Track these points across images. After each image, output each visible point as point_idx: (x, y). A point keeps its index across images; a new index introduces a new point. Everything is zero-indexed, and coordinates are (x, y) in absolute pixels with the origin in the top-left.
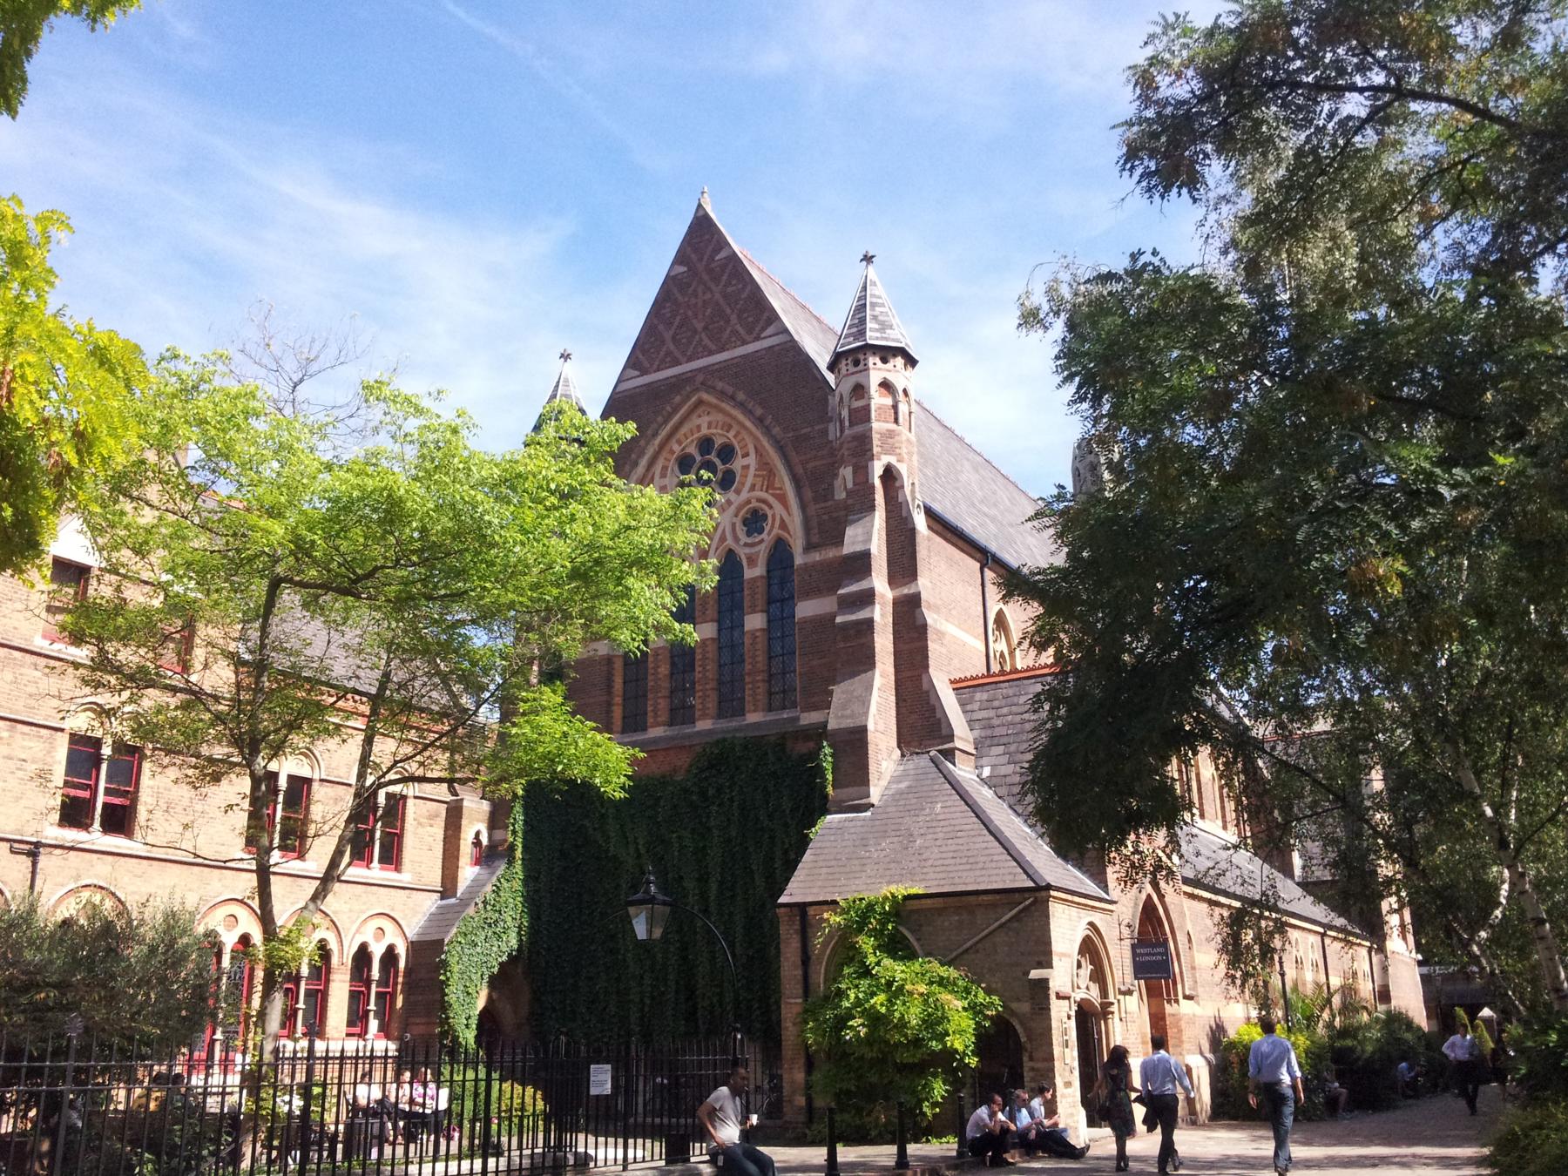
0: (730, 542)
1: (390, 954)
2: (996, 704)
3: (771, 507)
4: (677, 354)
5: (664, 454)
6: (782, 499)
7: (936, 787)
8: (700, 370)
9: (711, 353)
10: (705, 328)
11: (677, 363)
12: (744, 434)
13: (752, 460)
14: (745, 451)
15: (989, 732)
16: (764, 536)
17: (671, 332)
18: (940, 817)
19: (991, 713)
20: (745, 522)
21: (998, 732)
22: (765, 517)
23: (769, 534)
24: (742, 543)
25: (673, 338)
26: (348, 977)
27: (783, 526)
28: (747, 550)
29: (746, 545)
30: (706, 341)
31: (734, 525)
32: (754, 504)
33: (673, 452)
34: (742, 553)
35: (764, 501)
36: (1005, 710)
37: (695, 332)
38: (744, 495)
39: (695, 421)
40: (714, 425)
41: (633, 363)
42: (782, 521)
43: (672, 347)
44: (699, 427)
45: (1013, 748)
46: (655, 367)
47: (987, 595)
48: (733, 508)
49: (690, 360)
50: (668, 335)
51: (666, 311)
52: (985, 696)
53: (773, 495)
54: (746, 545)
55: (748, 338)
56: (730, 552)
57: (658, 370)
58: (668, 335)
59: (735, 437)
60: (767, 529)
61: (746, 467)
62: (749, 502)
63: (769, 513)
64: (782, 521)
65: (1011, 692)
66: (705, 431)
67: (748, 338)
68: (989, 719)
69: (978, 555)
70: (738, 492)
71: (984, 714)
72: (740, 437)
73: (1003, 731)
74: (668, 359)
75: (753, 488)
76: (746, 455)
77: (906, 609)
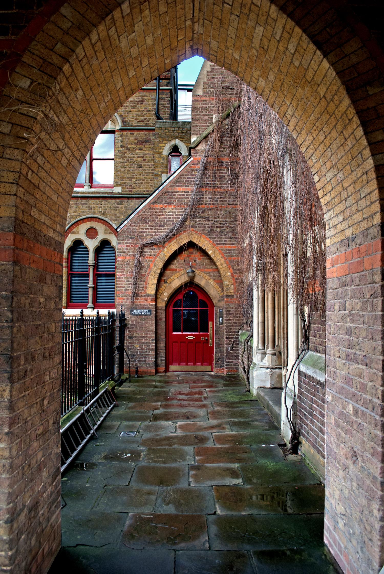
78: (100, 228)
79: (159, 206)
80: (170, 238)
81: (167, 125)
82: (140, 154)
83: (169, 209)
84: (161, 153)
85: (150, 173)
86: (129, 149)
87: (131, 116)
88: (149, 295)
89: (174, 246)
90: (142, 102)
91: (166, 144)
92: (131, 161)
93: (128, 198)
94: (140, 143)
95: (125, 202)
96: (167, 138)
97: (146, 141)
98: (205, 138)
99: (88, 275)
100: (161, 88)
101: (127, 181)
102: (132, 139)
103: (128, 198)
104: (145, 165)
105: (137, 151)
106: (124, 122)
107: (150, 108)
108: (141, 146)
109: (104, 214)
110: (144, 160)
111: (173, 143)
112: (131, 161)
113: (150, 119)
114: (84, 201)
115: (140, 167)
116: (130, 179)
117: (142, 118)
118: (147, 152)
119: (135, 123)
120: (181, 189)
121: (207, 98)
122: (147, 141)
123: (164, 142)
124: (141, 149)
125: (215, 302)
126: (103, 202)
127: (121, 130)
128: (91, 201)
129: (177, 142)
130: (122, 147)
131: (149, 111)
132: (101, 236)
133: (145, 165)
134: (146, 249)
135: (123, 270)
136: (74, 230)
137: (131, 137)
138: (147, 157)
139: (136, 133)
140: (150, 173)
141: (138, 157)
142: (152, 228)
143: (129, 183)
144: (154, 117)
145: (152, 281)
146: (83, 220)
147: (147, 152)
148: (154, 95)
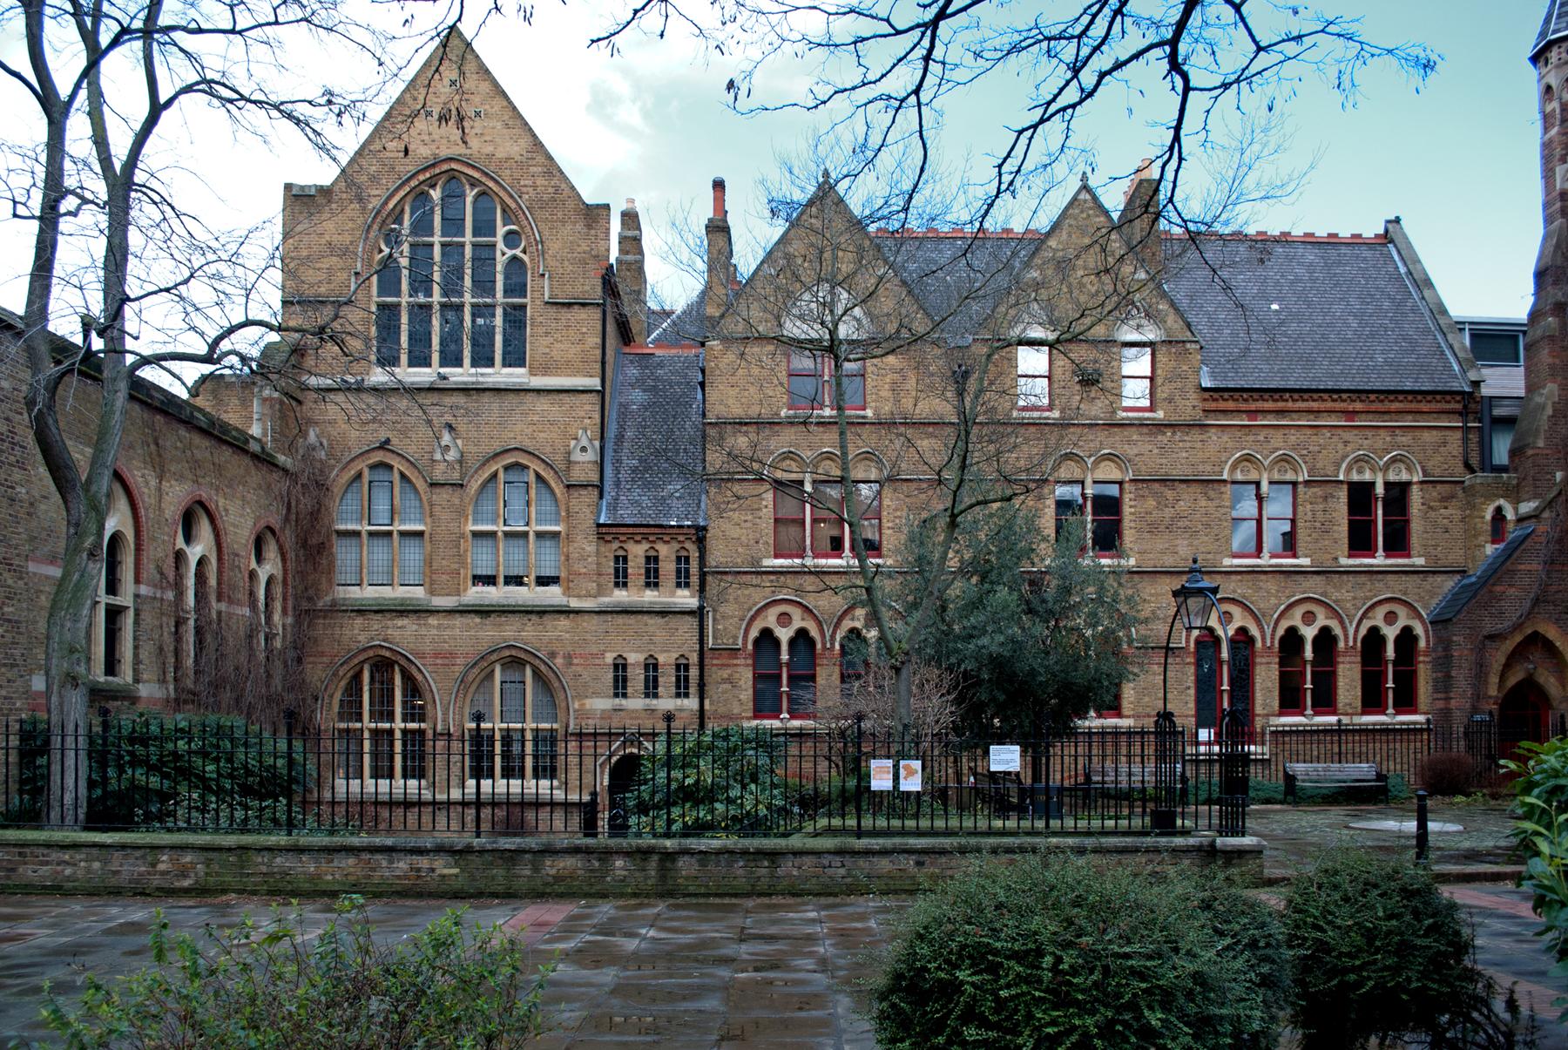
1: (1406, 637)
26: (1359, 659)
78: (1401, 611)
79: (1498, 588)
80: (1517, 627)
81: (1490, 480)
83: (1512, 591)
84: (1483, 517)
86: (1431, 508)
87: (1431, 463)
88: (1490, 697)
89: (1518, 638)
90: (1445, 444)
92: (1435, 524)
93: (1434, 573)
94: (1445, 499)
95: (1430, 579)
96: (1490, 497)
98: (1550, 502)
99: (779, 676)
101: (1431, 549)
102: (1435, 494)
103: (1434, 573)
106: (1425, 473)
107: (1455, 453)
109: (1405, 594)
111: (1497, 504)
112: (1435, 524)
114: (1380, 576)
116: (1436, 546)
119: (1437, 471)
120: (1523, 567)
121: (1548, 452)
124: (1446, 508)
125: (1555, 704)
126: (1404, 578)
127: (1422, 482)
128: (1390, 577)
129: (1502, 502)
130: (1423, 504)
132: (1401, 623)
134: (1487, 642)
135: (1460, 667)
136: (1370, 615)
137: (1434, 492)
139: (1439, 487)
142: (1491, 615)
143: (1434, 552)
144: (1461, 465)
145: (1494, 680)
146: (1380, 602)
148: (1459, 435)
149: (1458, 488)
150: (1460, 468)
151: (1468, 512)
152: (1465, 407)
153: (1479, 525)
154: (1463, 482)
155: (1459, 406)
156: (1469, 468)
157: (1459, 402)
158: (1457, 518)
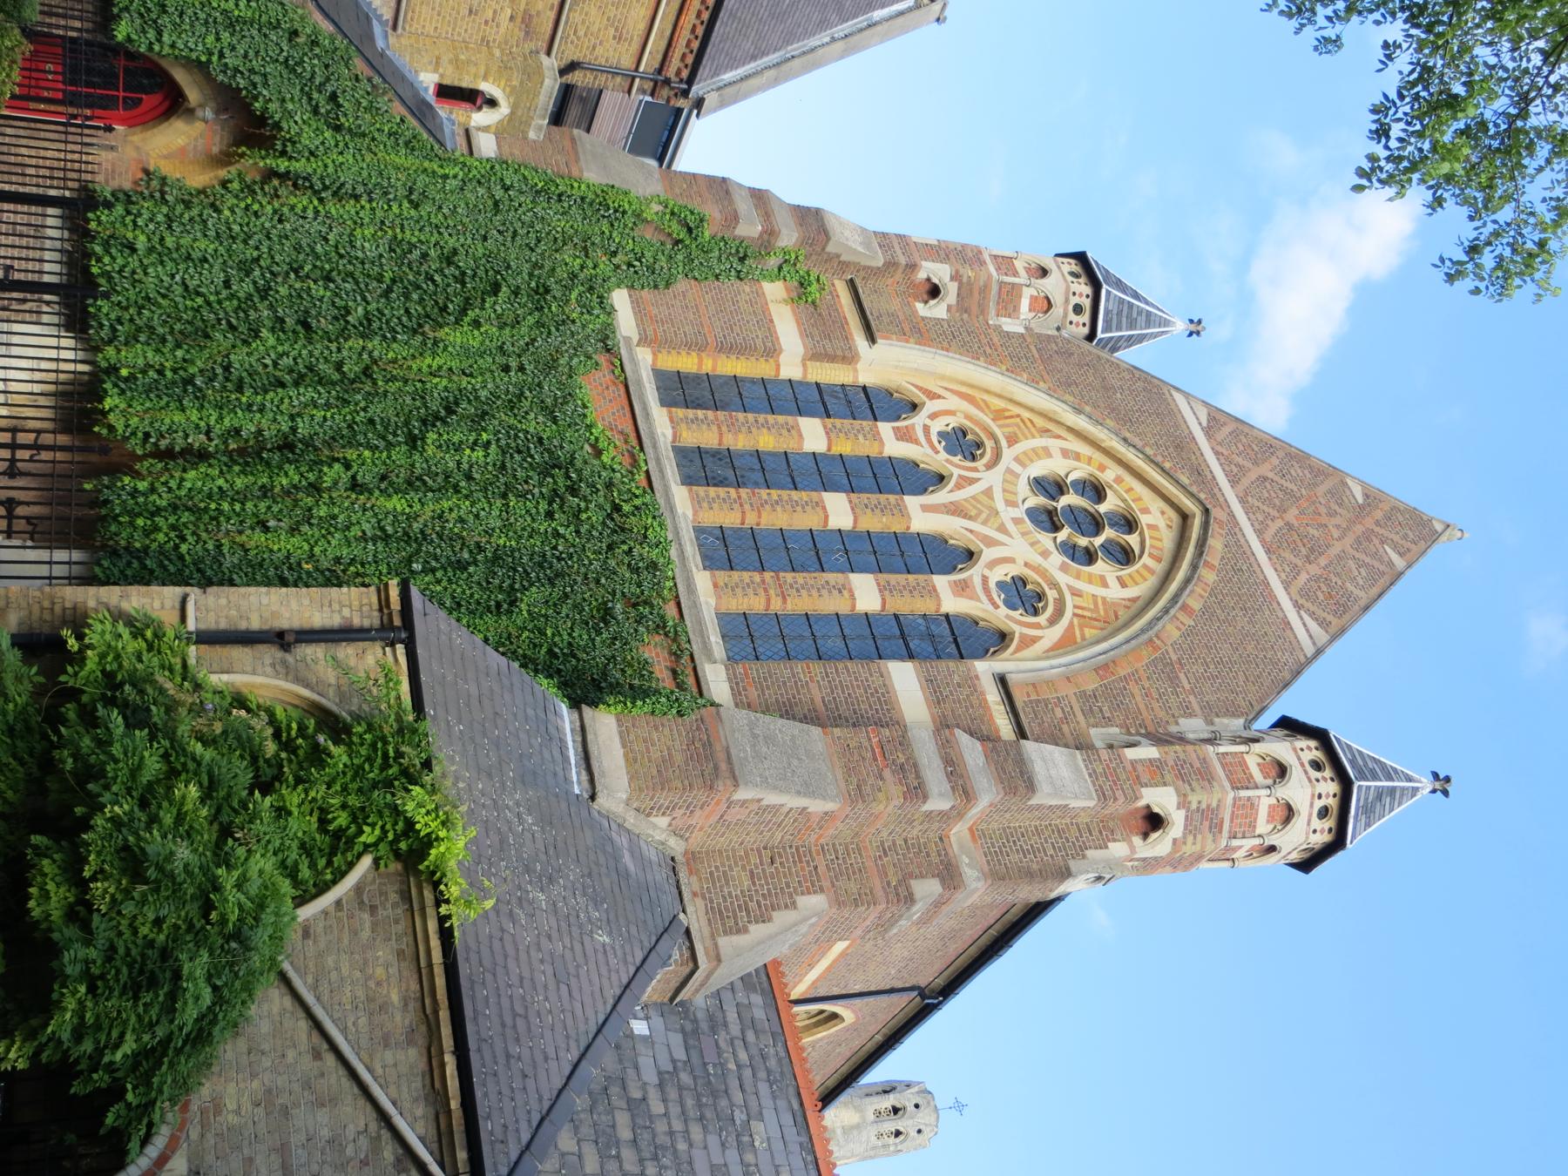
0: (988, 554)
2: (750, 1036)
3: (1053, 621)
4: (1245, 482)
5: (1098, 457)
6: (1067, 643)
7: (633, 930)
8: (1231, 515)
9: (1259, 533)
10: (1289, 526)
11: (1234, 482)
12: (1151, 582)
13: (1115, 593)
14: (1128, 581)
15: (704, 1026)
16: (1004, 610)
17: (1271, 475)
18: (587, 939)
19: (735, 1029)
20: (1020, 581)
21: (707, 1042)
22: (1036, 612)
23: (1007, 616)
24: (987, 572)
25: (1265, 479)
27: (1028, 642)
28: (977, 581)
29: (985, 580)
30: (1274, 527)
31: (1010, 560)
32: (1051, 595)
33: (1102, 468)
34: (974, 573)
35: (1059, 612)
36: (743, 1056)
37: (1283, 510)
38: (1063, 579)
39: (1156, 505)
40: (1155, 534)
41: (1217, 420)
42: (1034, 640)
43: (1253, 476)
44: (1146, 511)
45: (685, 1078)
46: (1219, 448)
47: (871, 999)
48: (1039, 560)
49: (1243, 501)
50: (1265, 470)
51: (1296, 471)
52: (759, 1014)
53: (1071, 624)
54: (985, 580)
55: (1294, 590)
56: (970, 555)
57: (1217, 453)
58: (1265, 470)
59: (1145, 566)
60: (1016, 614)
61: (1105, 584)
62: (1054, 585)
63: (1042, 619)
64: (1034, 640)
65: (772, 1063)
66: (1144, 520)
67: (1294, 590)
68: (725, 1025)
69: (941, 982)
70: (1064, 568)
71: (732, 1016)
72: (1145, 573)
73: (710, 1056)
74: (1235, 470)
75: (1076, 593)
76: (1123, 585)
77: (935, 859)
82: (503, 15)
84: (485, 78)
85: (454, 30)
91: (504, 90)
97: (529, 33)
100: (637, 80)
104: (474, 21)
105: (509, 11)
107: (599, 51)
108: (519, 20)
110: (486, 22)
113: (576, 47)
115: (471, 11)
117: (581, 33)
118: (502, 30)
122: (527, 33)
123: (508, 89)
124: (512, 18)
131: (594, 48)
133: (474, 21)
138: (491, 27)
140: (454, 30)
141: (495, 12)
147: (502, 30)
148: (627, 62)
149: (542, 45)
150: (572, 54)
151: (497, 53)
152: (667, 82)
153: (473, 70)
154: (549, 53)
155: (671, 72)
156: (572, 67)
157: (678, 73)
158: (490, 32)
